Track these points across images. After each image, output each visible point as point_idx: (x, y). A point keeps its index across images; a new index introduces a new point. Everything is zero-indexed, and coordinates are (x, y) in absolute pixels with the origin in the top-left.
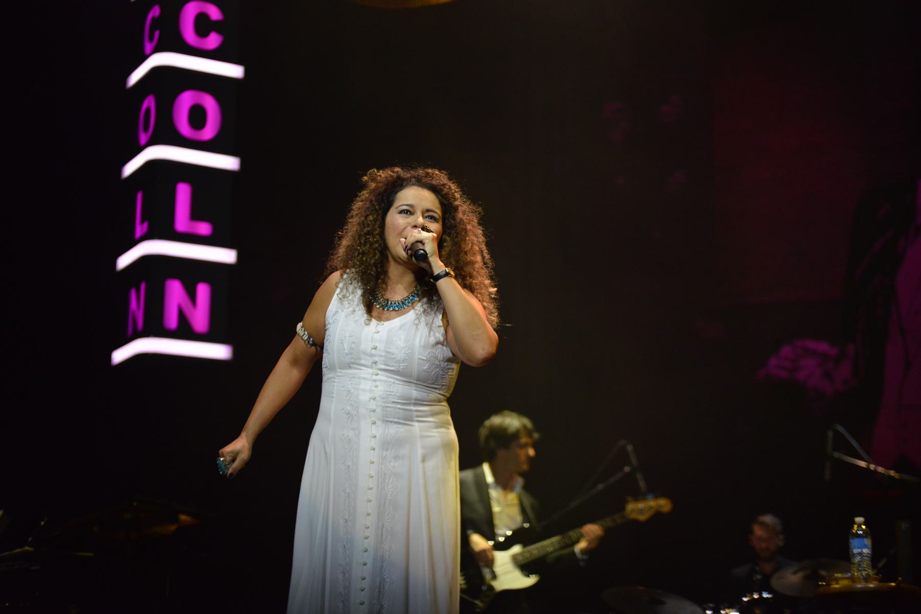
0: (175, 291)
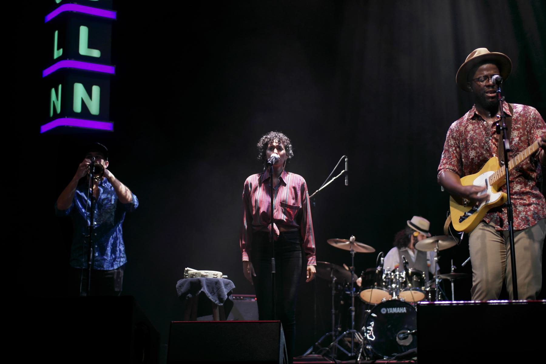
0: (79, 89)
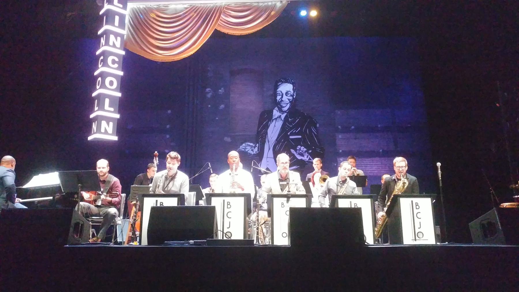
0: (104, 124)
